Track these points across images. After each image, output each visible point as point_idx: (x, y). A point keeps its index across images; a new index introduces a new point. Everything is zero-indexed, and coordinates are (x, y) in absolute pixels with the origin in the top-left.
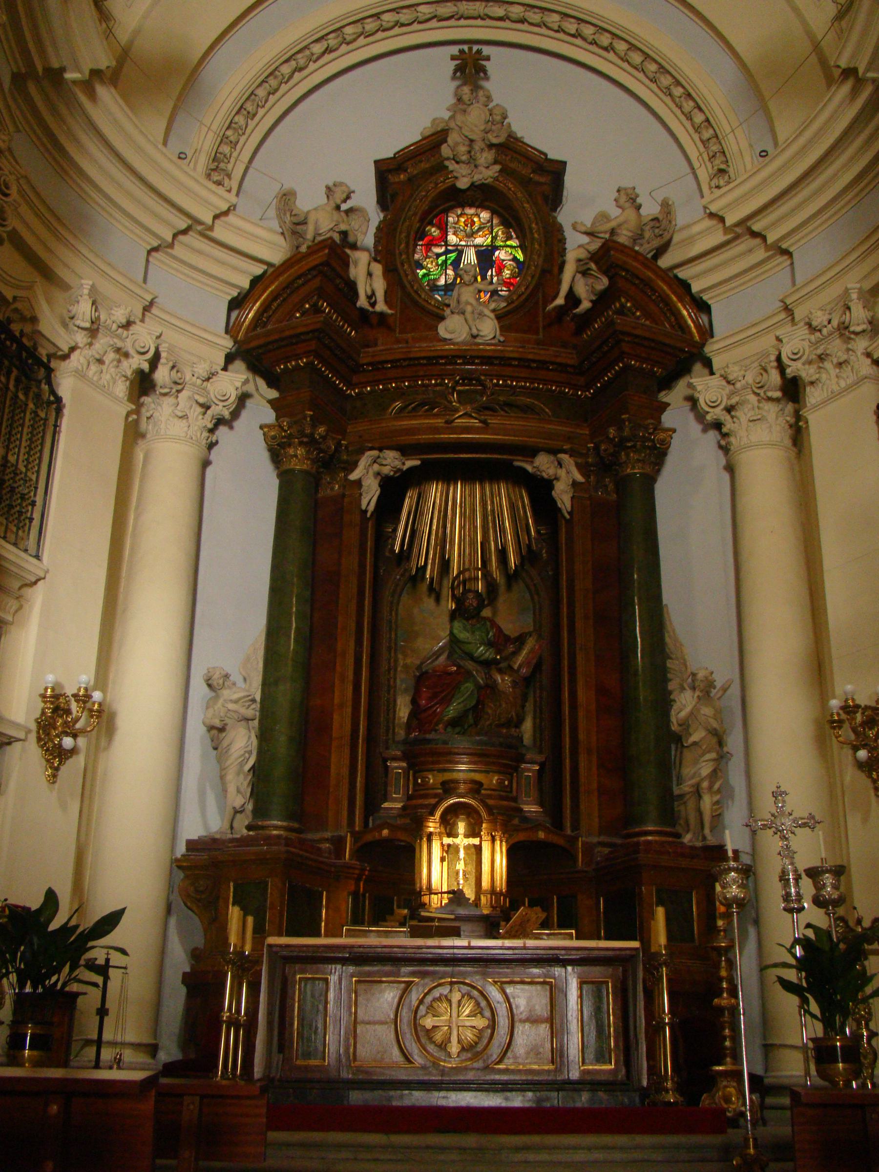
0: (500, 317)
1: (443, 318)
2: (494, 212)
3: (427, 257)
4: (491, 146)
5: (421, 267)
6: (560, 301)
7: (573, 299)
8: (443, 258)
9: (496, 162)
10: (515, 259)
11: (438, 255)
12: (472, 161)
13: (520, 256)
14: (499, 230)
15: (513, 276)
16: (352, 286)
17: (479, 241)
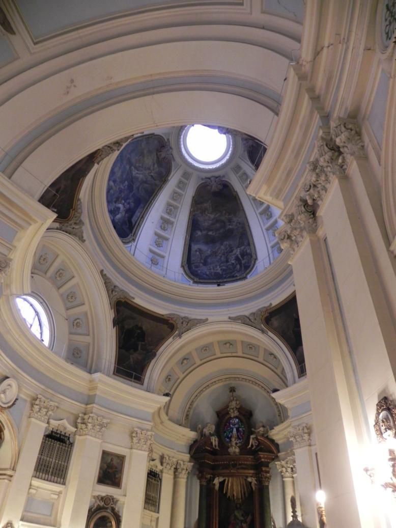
0: (239, 447)
1: (228, 448)
2: (239, 419)
6: (250, 446)
7: (252, 446)
12: (234, 411)
14: (240, 424)
15: (243, 434)
16: (212, 443)
17: (236, 426)
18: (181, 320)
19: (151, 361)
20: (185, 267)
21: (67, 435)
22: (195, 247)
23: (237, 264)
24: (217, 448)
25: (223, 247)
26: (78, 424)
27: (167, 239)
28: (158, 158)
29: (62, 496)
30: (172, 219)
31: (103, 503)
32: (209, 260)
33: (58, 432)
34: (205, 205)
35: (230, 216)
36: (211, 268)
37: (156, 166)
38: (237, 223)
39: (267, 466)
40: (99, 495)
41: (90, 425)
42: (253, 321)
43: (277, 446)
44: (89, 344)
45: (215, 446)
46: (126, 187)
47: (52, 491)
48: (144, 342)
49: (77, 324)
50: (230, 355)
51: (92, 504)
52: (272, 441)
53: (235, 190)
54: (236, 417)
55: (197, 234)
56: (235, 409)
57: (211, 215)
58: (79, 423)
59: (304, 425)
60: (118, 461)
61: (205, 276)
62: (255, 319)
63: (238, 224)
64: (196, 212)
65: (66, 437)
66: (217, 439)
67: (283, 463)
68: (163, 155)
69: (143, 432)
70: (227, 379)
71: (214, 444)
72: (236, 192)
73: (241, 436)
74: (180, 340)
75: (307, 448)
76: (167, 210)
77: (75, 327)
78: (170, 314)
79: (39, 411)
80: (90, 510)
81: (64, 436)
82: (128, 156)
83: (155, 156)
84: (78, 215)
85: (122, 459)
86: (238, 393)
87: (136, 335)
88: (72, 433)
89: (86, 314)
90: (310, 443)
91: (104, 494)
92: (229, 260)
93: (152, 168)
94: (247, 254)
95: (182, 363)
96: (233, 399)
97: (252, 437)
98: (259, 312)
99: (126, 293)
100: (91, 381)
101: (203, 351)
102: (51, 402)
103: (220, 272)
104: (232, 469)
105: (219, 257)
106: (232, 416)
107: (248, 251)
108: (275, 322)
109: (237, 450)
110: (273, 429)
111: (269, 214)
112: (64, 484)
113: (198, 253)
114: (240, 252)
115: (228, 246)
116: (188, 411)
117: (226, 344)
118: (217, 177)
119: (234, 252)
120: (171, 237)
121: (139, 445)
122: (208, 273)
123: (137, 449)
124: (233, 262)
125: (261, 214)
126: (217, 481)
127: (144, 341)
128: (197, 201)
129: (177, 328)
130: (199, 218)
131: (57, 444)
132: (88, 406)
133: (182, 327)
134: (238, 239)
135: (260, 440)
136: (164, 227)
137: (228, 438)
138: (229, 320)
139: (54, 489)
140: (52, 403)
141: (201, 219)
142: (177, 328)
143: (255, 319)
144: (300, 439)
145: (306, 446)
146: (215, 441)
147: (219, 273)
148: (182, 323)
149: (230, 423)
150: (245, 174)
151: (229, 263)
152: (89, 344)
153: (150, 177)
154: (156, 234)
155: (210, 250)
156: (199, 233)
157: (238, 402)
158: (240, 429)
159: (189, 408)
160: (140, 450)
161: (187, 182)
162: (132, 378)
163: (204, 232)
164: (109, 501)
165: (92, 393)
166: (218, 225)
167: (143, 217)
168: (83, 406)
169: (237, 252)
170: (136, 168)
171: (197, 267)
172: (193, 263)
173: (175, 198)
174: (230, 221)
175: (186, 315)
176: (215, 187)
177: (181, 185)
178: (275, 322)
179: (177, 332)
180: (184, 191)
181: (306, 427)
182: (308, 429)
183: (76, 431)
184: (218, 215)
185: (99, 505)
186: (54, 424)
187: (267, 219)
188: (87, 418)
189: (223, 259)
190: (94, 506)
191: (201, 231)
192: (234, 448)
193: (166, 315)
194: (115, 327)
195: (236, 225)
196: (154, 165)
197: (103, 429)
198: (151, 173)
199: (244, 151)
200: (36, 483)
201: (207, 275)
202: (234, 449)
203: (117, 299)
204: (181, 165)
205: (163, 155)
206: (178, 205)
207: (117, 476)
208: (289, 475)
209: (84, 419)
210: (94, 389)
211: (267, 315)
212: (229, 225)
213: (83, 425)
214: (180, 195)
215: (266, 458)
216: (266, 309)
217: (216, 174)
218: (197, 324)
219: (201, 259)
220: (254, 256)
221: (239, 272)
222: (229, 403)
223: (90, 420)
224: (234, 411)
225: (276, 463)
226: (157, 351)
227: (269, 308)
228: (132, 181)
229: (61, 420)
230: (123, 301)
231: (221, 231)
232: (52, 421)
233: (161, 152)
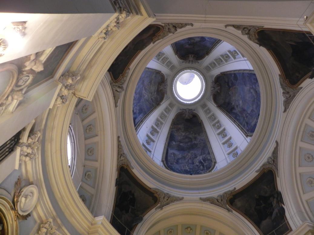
18: (164, 195)
19: (137, 224)
20: (164, 162)
22: (171, 151)
23: (200, 166)
25: (190, 154)
27: (154, 141)
28: (158, 89)
30: (158, 130)
32: (180, 161)
34: (180, 126)
35: (195, 136)
36: (182, 166)
37: (155, 93)
38: (200, 140)
42: (220, 201)
46: (137, 98)
49: (88, 175)
53: (201, 119)
55: (173, 143)
57: (182, 133)
61: (178, 171)
63: (201, 141)
64: (174, 130)
68: (162, 88)
72: (202, 120)
76: (156, 123)
78: (156, 189)
82: (144, 79)
83: (157, 87)
84: (123, 81)
87: (129, 199)
89: (96, 170)
92: (195, 163)
93: (153, 94)
94: (208, 160)
98: (225, 195)
99: (129, 162)
101: (169, 232)
103: (189, 170)
105: (187, 160)
107: (209, 158)
108: (239, 203)
111: (225, 134)
113: (172, 155)
114: (202, 158)
115: (193, 154)
117: (187, 228)
118: (190, 110)
119: (198, 158)
120: (156, 141)
122: (179, 169)
124: (198, 164)
125: (219, 134)
128: (175, 123)
130: (175, 134)
134: (201, 151)
136: (153, 133)
138: (200, 200)
141: (176, 134)
143: (222, 200)
147: (187, 170)
148: (164, 198)
150: (209, 109)
151: (195, 165)
153: (151, 99)
154: (147, 136)
155: (180, 155)
156: (174, 143)
161: (171, 109)
163: (177, 143)
166: (187, 140)
167: (142, 121)
169: (200, 158)
170: (145, 89)
171: (172, 164)
172: (169, 161)
173: (162, 117)
174: (195, 138)
175: (167, 192)
176: (187, 117)
177: (167, 110)
178: (239, 203)
179: (159, 205)
180: (168, 114)
184: (187, 134)
187: (223, 138)
189: (190, 161)
191: (175, 142)
193: (153, 188)
195: (200, 141)
196: (155, 92)
198: (152, 96)
199: (211, 95)
201: (179, 170)
203: (122, 164)
204: (170, 98)
205: (162, 88)
206: (163, 122)
211: (231, 197)
212: (195, 141)
214: (166, 116)
216: (231, 192)
217: (190, 108)
218: (175, 200)
219: (174, 159)
220: (213, 161)
221: (203, 170)
226: (144, 216)
227: (233, 192)
228: (141, 96)
230: (126, 167)
231: (189, 144)
233: (161, 85)
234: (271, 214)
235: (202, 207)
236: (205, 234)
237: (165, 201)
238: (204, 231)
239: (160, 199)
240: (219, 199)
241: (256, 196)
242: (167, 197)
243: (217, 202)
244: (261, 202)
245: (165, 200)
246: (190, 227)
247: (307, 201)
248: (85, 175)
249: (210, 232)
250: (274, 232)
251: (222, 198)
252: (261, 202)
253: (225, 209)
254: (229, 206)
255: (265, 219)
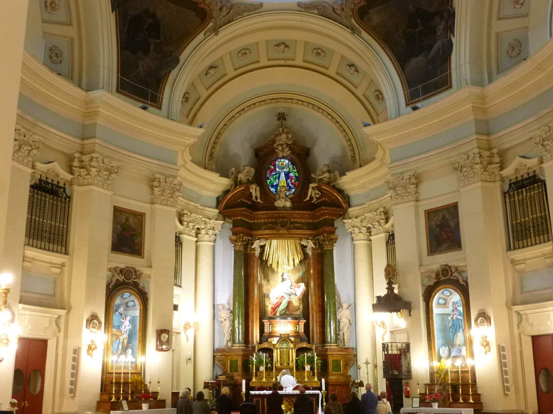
1: (276, 200)
3: (270, 176)
4: (288, 145)
5: (269, 179)
6: (308, 198)
7: (311, 198)
8: (275, 176)
9: (290, 150)
10: (295, 176)
11: (274, 175)
12: (283, 149)
13: (297, 175)
14: (291, 166)
15: (295, 182)
16: (251, 193)
17: (285, 170)
19: (170, 72)
21: (61, 185)
24: (259, 200)
26: (73, 168)
29: (66, 270)
31: (123, 278)
33: (49, 181)
39: (333, 225)
40: (117, 267)
41: (94, 170)
42: (338, 12)
43: (347, 199)
44: (72, 39)
45: (256, 198)
47: (51, 263)
48: (158, 37)
50: (282, 62)
51: (109, 279)
52: (340, 191)
54: (283, 157)
56: (284, 146)
58: (76, 167)
59: (411, 173)
60: (136, 221)
62: (343, 10)
65: (61, 187)
66: (258, 189)
67: (357, 222)
69: (168, 180)
70: (274, 101)
71: (254, 195)
73: (292, 183)
74: (216, 38)
75: (413, 203)
77: (49, 10)
79: (19, 149)
80: (108, 286)
81: (58, 186)
85: (139, 217)
86: (289, 122)
87: (146, 26)
88: (68, 181)
90: (417, 197)
91: (122, 266)
95: (206, 74)
96: (283, 132)
97: (311, 185)
100: (88, 103)
101: (240, 55)
102: (34, 136)
104: (280, 229)
106: (280, 156)
109: (288, 204)
110: (344, 175)
112: (66, 253)
116: (213, 148)
121: (163, 198)
123: (160, 204)
126: (256, 245)
127: (158, 37)
129: (212, 18)
131: (48, 198)
132: (86, 142)
133: (220, 16)
135: (322, 190)
137: (272, 186)
138: (299, 9)
139: (54, 261)
140: (36, 138)
142: (212, 18)
143: (343, 10)
144: (403, 191)
145: (412, 201)
146: (255, 191)
148: (221, 9)
149: (275, 166)
152: (72, 39)
157: (290, 136)
158: (291, 174)
159: (214, 143)
160: (165, 205)
162: (147, 100)
164: (131, 276)
165: (87, 122)
168: (79, 141)
181: (414, 175)
182: (416, 179)
183: (72, 179)
185: (117, 279)
186: (41, 167)
188: (87, 160)
190: (112, 282)
192: (283, 200)
194: (114, 12)
197: (113, 175)
200: (32, 253)
202: (283, 203)
207: (136, 241)
208: (362, 236)
209: (83, 161)
210: (96, 113)
213: (82, 170)
215: (329, 214)
222: (277, 136)
223: (93, 164)
224: (283, 149)
225: (345, 221)
226: (180, 55)
229: (50, 162)
232: (39, 165)
234: (431, 47)
235: (302, 21)
236: (315, 54)
237: (225, 16)
238: (313, 49)
239: (213, 12)
240: (337, 9)
241: (410, 7)
242: (227, 9)
243: (334, 14)
244: (419, 21)
245: (224, 13)
246: (284, 43)
247: (498, 35)
248: (44, 6)
249: (324, 52)
250: (419, 88)
251: (344, 6)
252: (419, 21)
253: (348, 27)
254: (356, 22)
255: (417, 56)
